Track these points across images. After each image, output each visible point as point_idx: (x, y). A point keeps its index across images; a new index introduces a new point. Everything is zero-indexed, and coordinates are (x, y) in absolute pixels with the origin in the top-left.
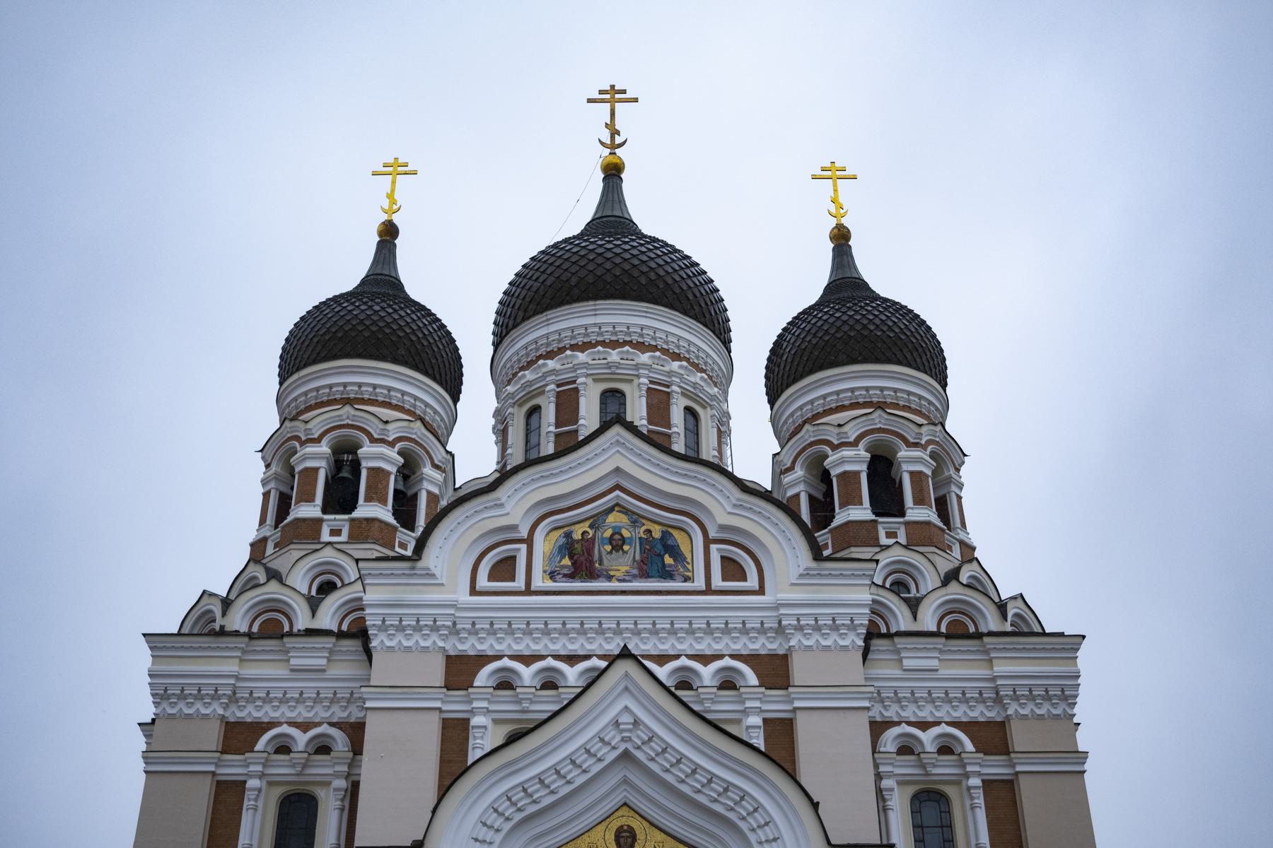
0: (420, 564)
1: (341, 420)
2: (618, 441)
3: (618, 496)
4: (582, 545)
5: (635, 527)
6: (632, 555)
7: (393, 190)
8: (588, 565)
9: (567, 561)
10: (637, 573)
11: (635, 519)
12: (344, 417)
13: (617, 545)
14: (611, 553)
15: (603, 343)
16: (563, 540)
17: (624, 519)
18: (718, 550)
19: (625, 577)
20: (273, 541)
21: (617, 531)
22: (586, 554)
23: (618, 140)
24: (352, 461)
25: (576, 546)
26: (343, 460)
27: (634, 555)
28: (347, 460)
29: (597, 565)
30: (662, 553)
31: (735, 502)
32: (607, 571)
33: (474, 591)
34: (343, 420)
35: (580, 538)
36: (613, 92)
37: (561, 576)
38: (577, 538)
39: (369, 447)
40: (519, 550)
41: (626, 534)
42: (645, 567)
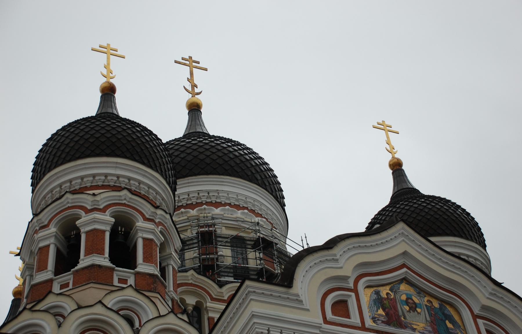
0: (291, 291)
1: (119, 200)
2: (402, 233)
3: (406, 272)
4: (389, 302)
5: (420, 296)
6: (424, 315)
7: (108, 64)
8: (396, 317)
9: (381, 312)
10: (431, 330)
11: (421, 291)
12: (123, 198)
13: (412, 307)
14: (409, 311)
15: (229, 205)
16: (375, 297)
17: (411, 291)
18: (484, 324)
19: (424, 331)
20: (58, 283)
21: (409, 297)
22: (393, 309)
23: (197, 90)
24: (124, 232)
25: (385, 302)
26: (118, 231)
27: (426, 317)
28: (121, 231)
29: (402, 319)
30: (444, 319)
31: (490, 291)
32: (411, 324)
33: (326, 321)
34: (122, 200)
35: (386, 297)
36: (191, 61)
37: (380, 322)
38: (383, 296)
39: (143, 223)
40: (350, 296)
41: (416, 300)
42: (435, 327)
